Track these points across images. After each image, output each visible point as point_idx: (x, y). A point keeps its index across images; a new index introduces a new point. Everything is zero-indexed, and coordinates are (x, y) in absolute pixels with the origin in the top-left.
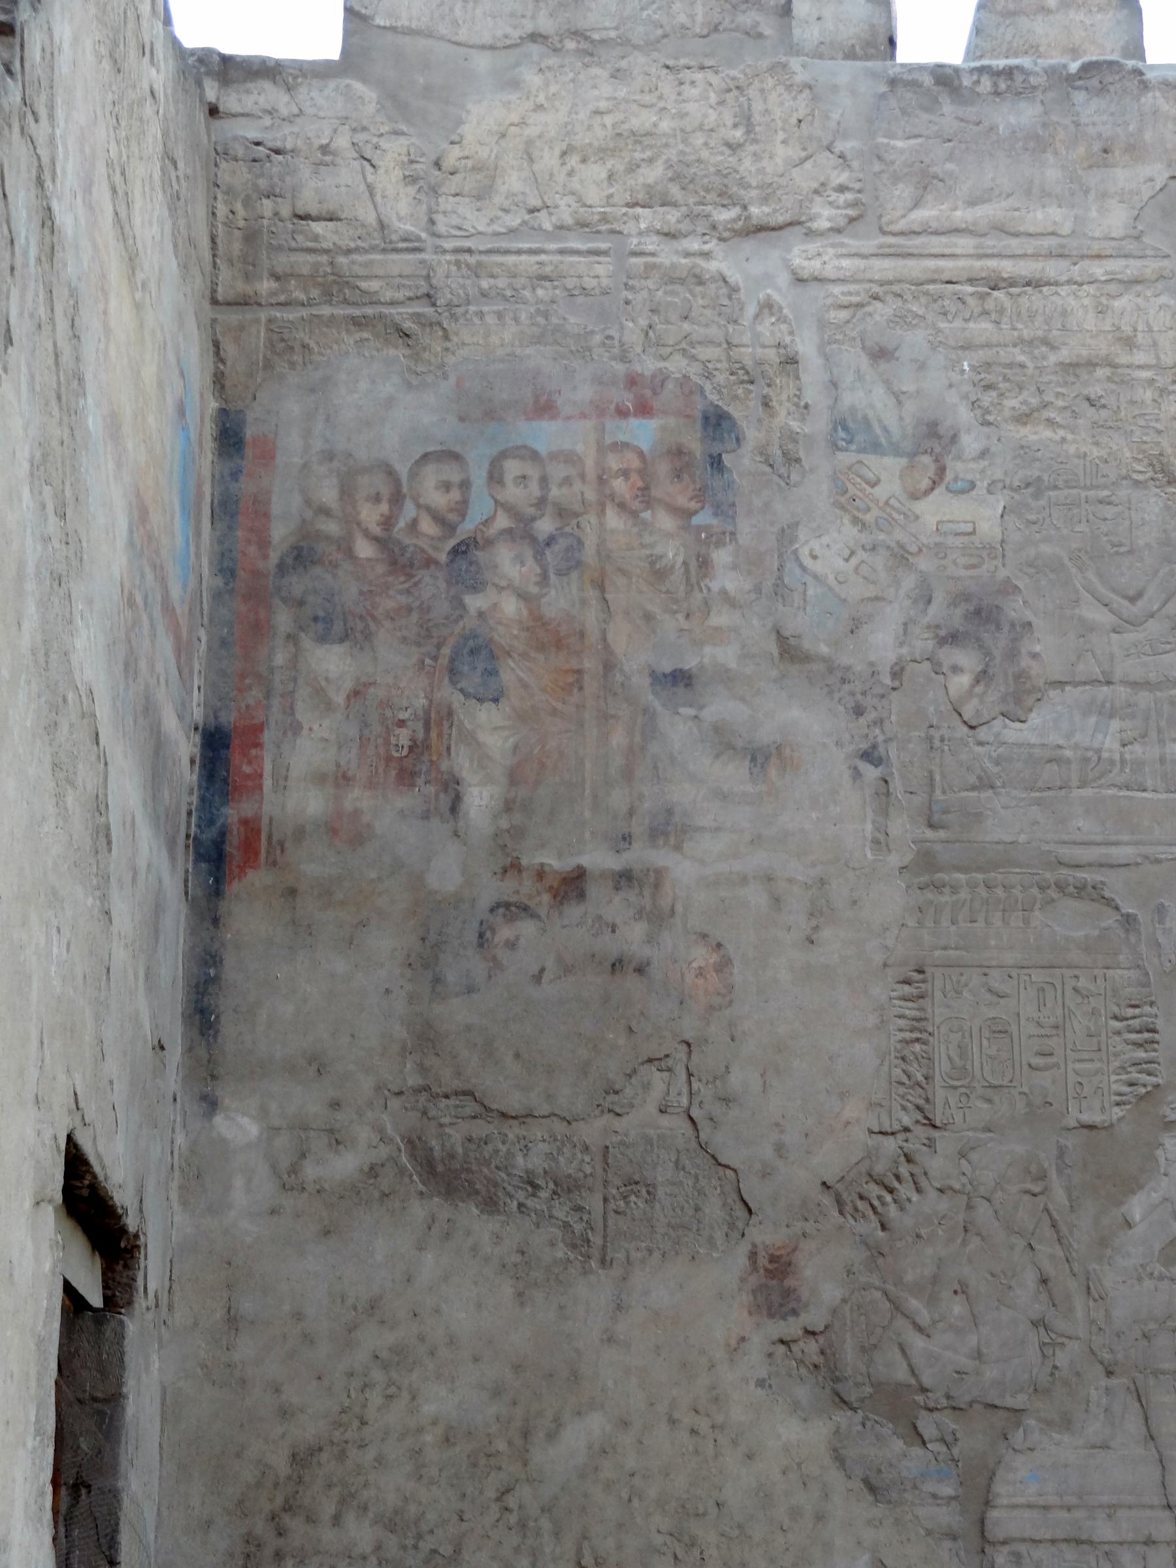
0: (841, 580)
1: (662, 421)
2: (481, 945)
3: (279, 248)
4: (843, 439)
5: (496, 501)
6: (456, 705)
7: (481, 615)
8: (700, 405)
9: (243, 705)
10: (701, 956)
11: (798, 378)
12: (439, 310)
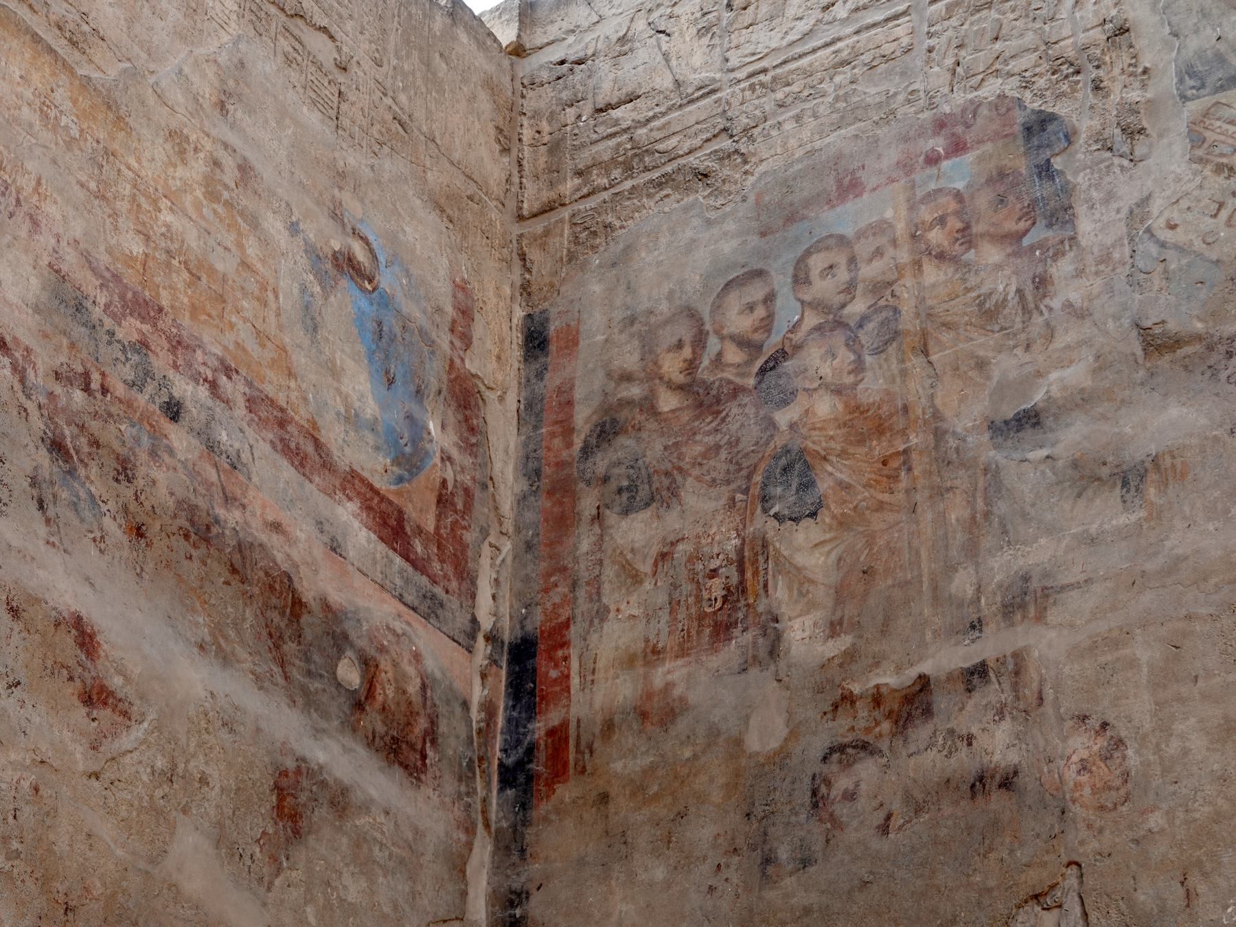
0: (1210, 240)
1: (978, 152)
2: (815, 806)
3: (583, 146)
4: (1193, 87)
5: (802, 302)
6: (770, 534)
7: (792, 426)
8: (1020, 117)
9: (549, 605)
10: (1082, 745)
11: (1131, 46)
12: (736, 138)
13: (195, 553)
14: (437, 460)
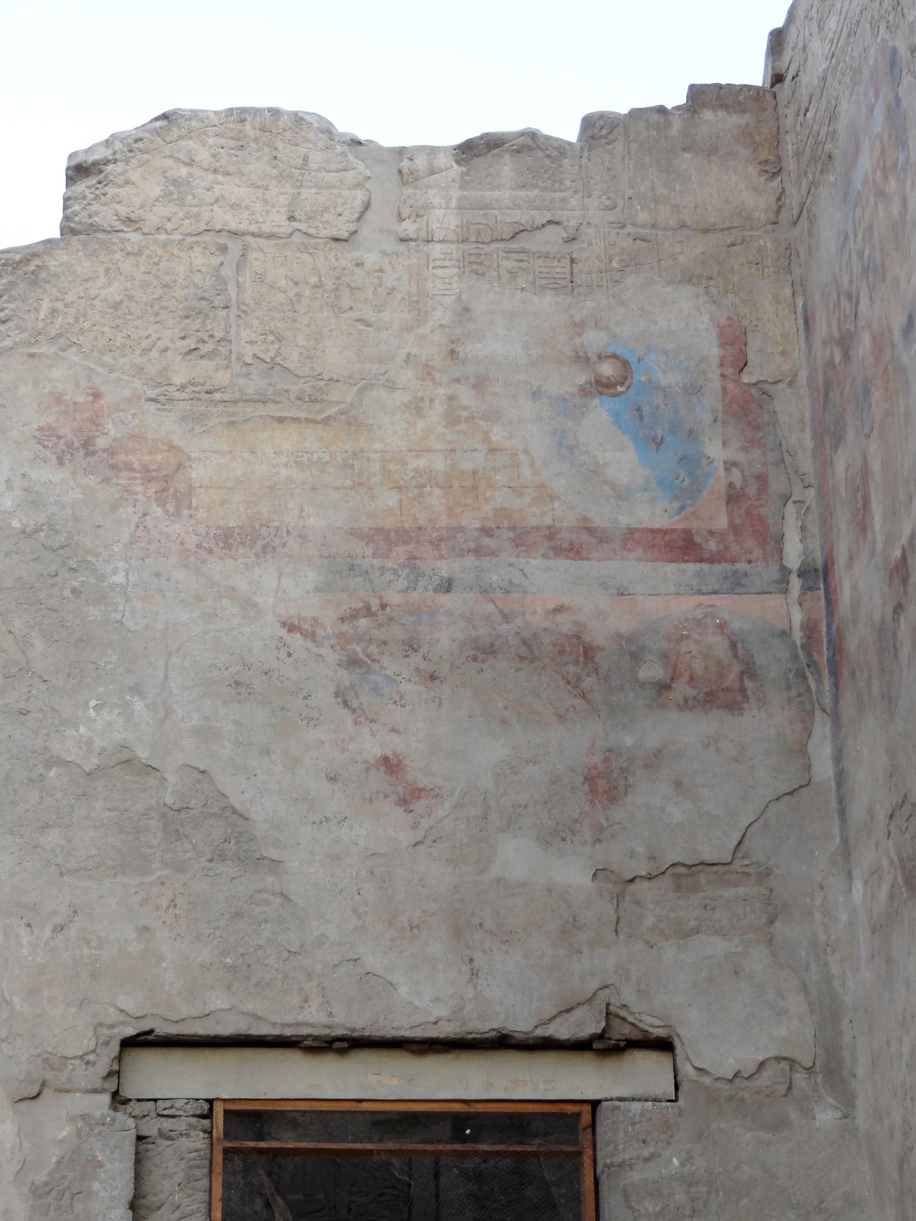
13: (484, 666)
14: (721, 472)
